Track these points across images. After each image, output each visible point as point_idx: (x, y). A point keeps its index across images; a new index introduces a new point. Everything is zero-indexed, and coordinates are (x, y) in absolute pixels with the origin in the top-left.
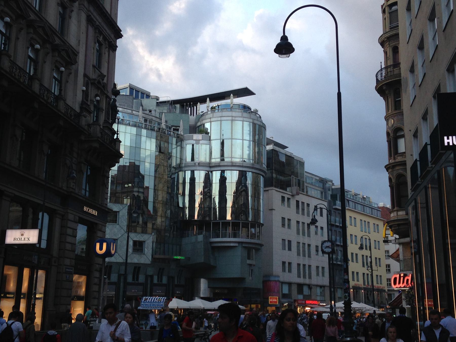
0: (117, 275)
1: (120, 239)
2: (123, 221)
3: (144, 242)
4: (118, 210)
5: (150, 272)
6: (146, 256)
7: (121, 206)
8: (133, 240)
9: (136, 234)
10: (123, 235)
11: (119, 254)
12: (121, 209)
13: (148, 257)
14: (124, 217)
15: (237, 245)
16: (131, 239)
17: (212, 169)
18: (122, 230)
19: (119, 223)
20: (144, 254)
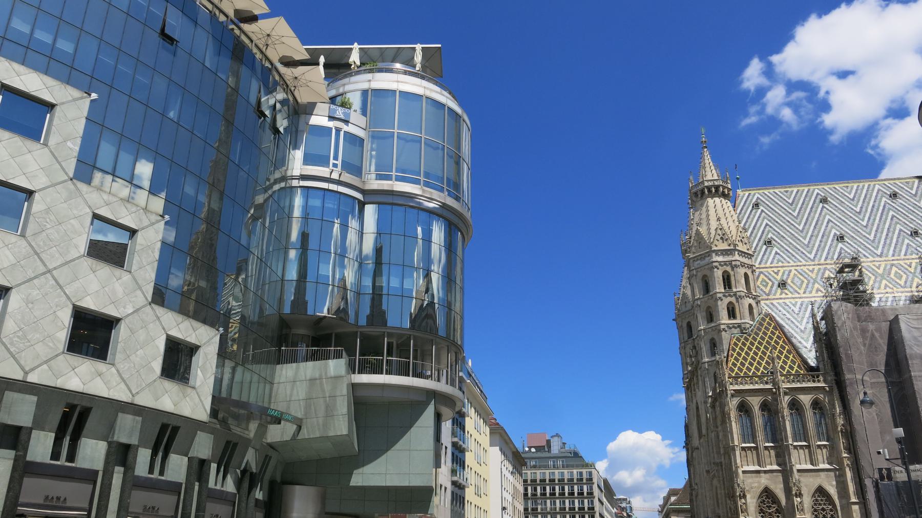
0: (102, 446)
1: (127, 320)
2: (145, 263)
3: (200, 347)
4: (133, 226)
6: (197, 393)
7: (144, 217)
8: (167, 334)
9: (180, 318)
11: (118, 371)
13: (203, 399)
14: (150, 252)
15: (423, 398)
16: (164, 329)
17: (368, 199)
18: (139, 293)
19: (134, 268)
20: (194, 388)
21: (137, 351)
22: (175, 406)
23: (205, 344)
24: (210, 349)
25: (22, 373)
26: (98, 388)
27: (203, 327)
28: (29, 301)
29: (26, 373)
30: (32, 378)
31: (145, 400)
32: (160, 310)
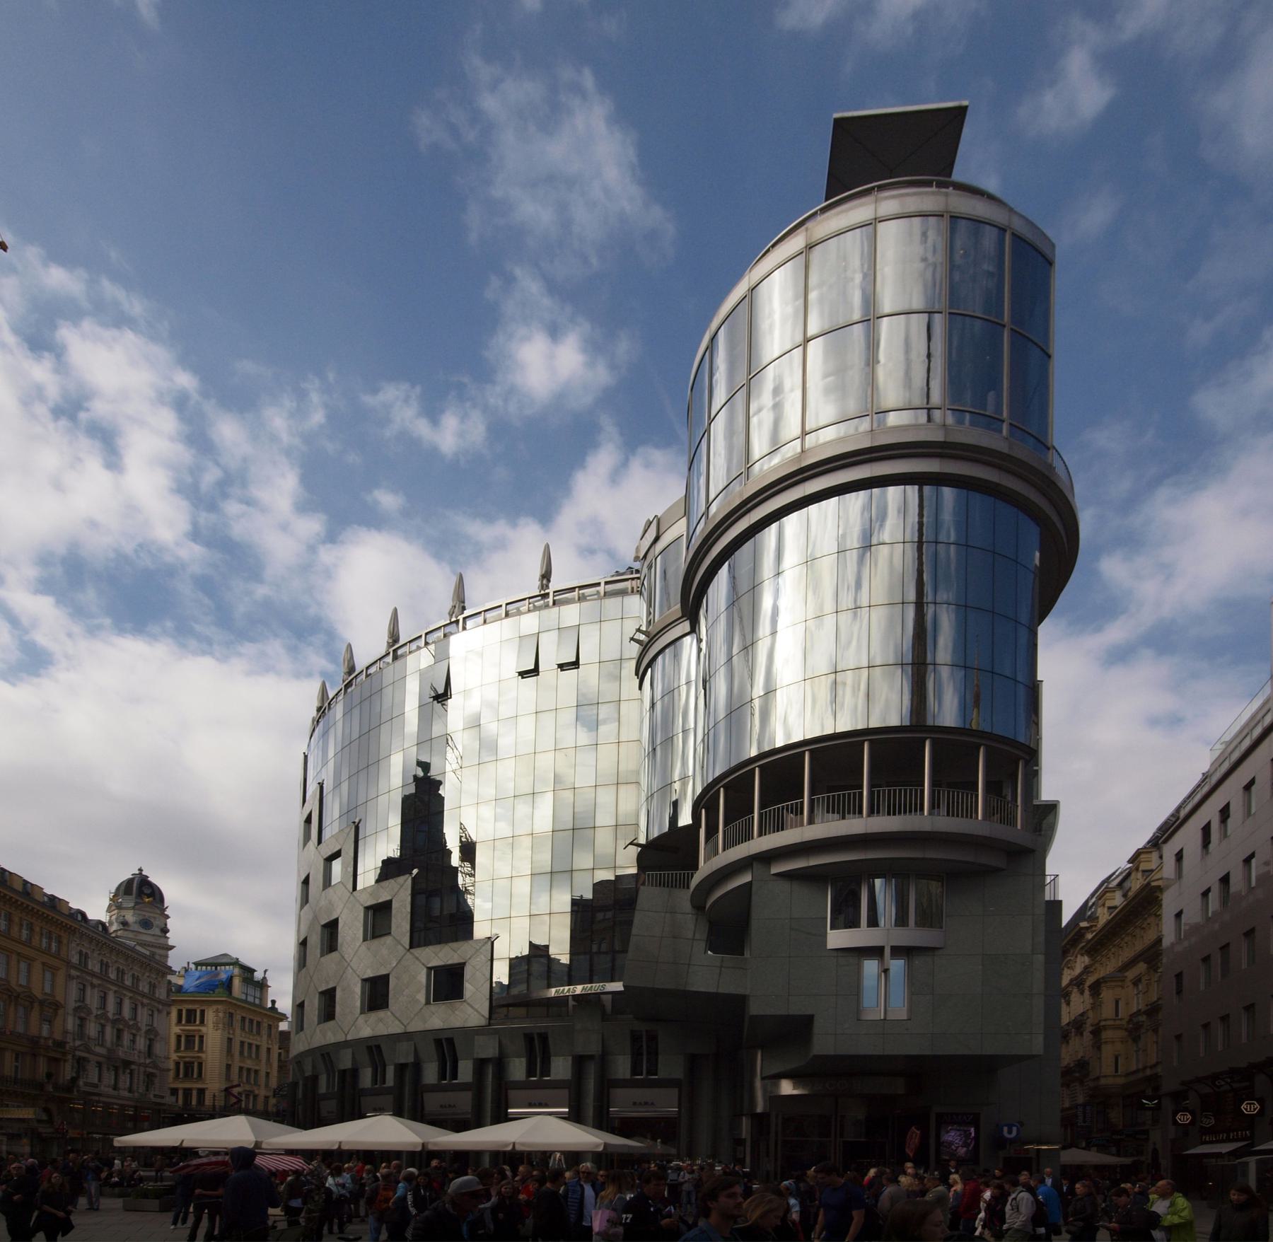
3: (464, 964)
5: (487, 1048)
6: (468, 1004)
10: (400, 960)
11: (392, 1013)
12: (396, 890)
13: (476, 1007)
14: (404, 910)
16: (423, 964)
18: (400, 947)
21: (404, 991)
22: (444, 1022)
23: (470, 958)
24: (478, 959)
25: (344, 1036)
26: (382, 1030)
27: (466, 944)
28: (343, 990)
29: (346, 1035)
30: (349, 1038)
31: (416, 1026)
32: (417, 951)
